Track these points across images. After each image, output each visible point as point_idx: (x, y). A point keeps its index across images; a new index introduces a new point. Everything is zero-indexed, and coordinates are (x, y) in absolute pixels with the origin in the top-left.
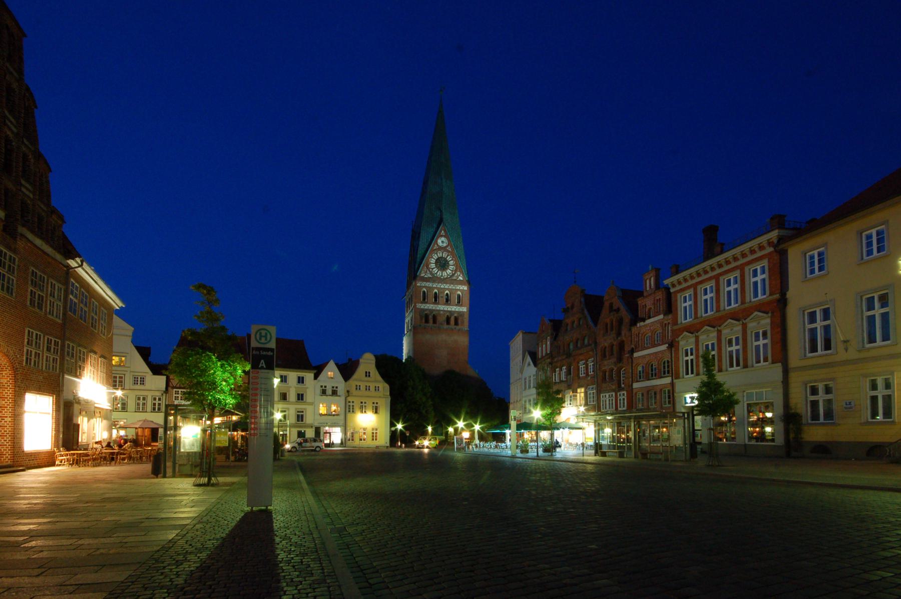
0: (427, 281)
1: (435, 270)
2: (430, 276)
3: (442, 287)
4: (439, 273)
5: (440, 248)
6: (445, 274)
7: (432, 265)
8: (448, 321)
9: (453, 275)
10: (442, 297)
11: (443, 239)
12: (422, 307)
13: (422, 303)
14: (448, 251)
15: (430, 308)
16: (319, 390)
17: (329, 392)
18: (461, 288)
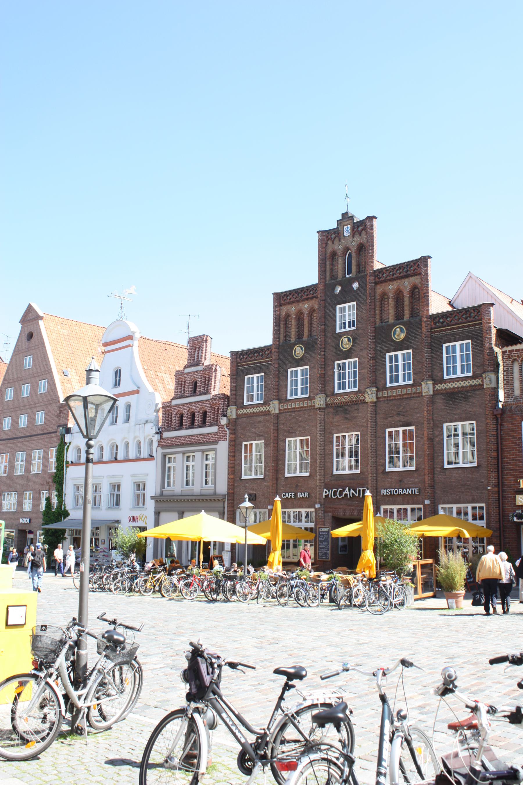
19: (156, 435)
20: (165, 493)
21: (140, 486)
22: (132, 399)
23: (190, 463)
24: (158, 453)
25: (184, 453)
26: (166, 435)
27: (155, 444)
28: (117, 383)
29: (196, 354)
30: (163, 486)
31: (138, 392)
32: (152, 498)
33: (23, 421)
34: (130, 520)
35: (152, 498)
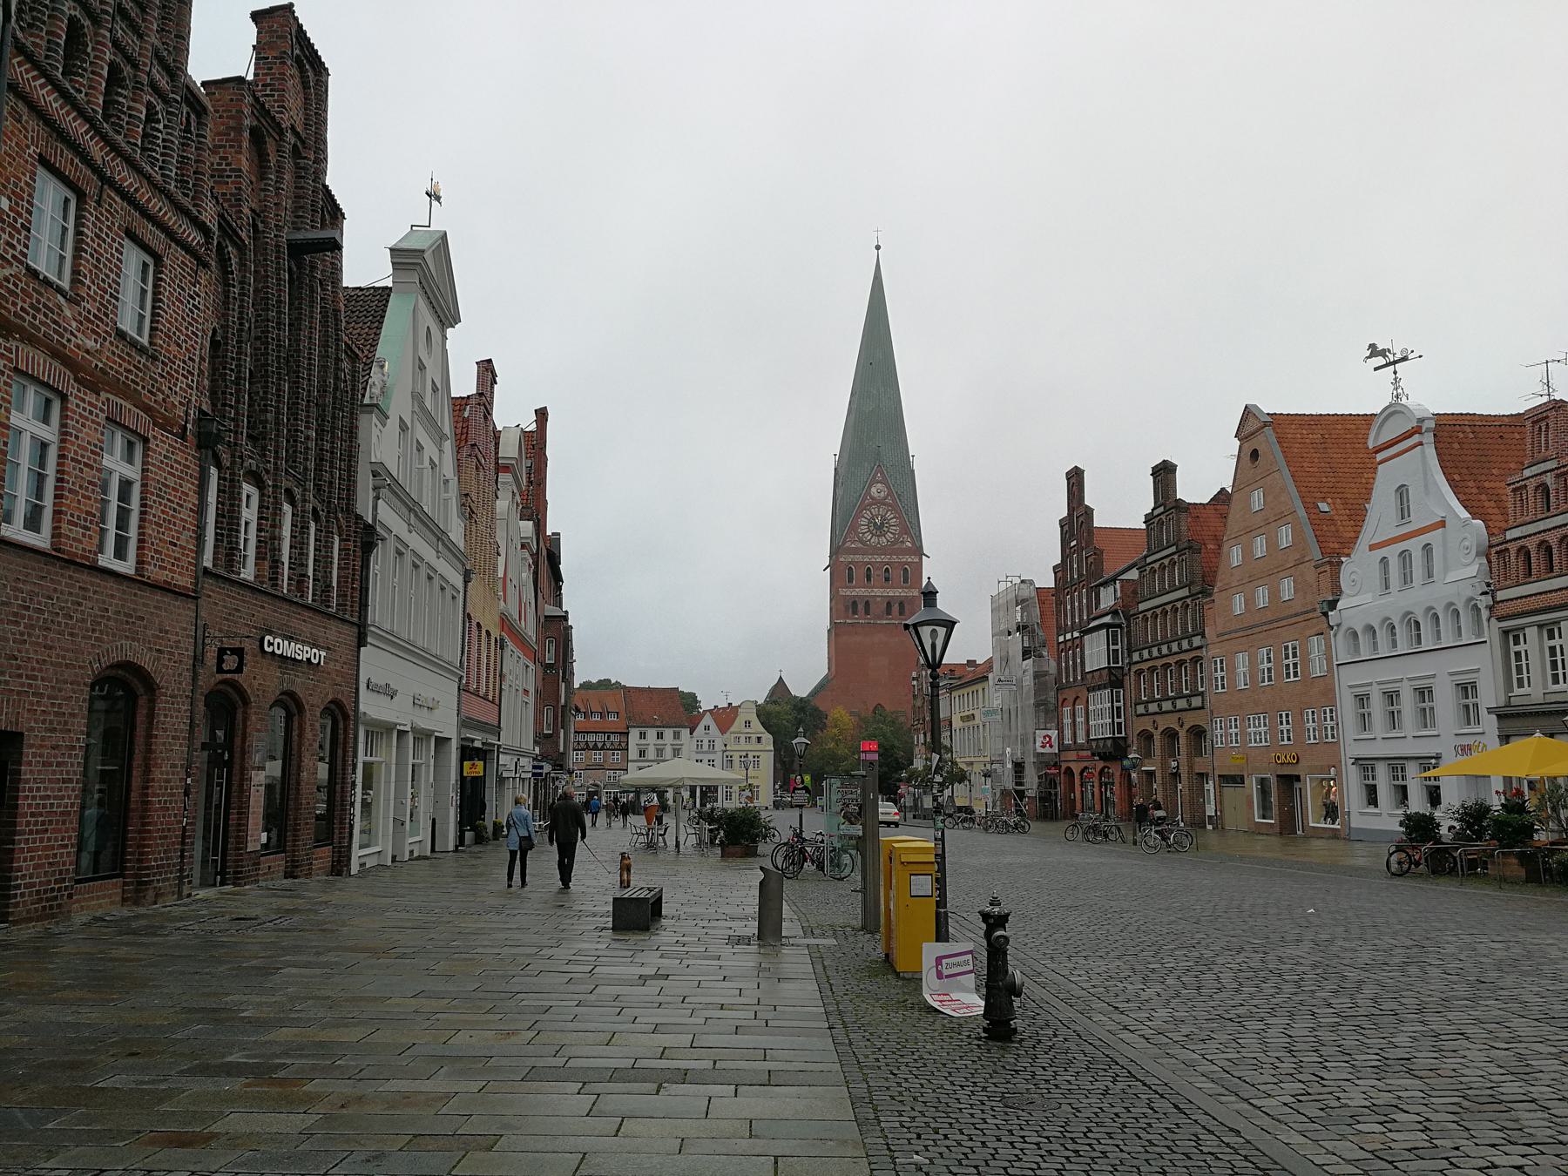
12: (848, 593)
19: (1483, 597)
20: (1514, 701)
21: (1467, 689)
22: (1434, 537)
23: (1556, 642)
24: (1492, 630)
25: (1540, 626)
26: (1500, 595)
27: (1485, 614)
28: (1404, 512)
29: (1543, 439)
30: (1509, 688)
31: (1442, 524)
32: (1490, 711)
33: (1262, 597)
34: (1457, 753)
35: (1490, 711)
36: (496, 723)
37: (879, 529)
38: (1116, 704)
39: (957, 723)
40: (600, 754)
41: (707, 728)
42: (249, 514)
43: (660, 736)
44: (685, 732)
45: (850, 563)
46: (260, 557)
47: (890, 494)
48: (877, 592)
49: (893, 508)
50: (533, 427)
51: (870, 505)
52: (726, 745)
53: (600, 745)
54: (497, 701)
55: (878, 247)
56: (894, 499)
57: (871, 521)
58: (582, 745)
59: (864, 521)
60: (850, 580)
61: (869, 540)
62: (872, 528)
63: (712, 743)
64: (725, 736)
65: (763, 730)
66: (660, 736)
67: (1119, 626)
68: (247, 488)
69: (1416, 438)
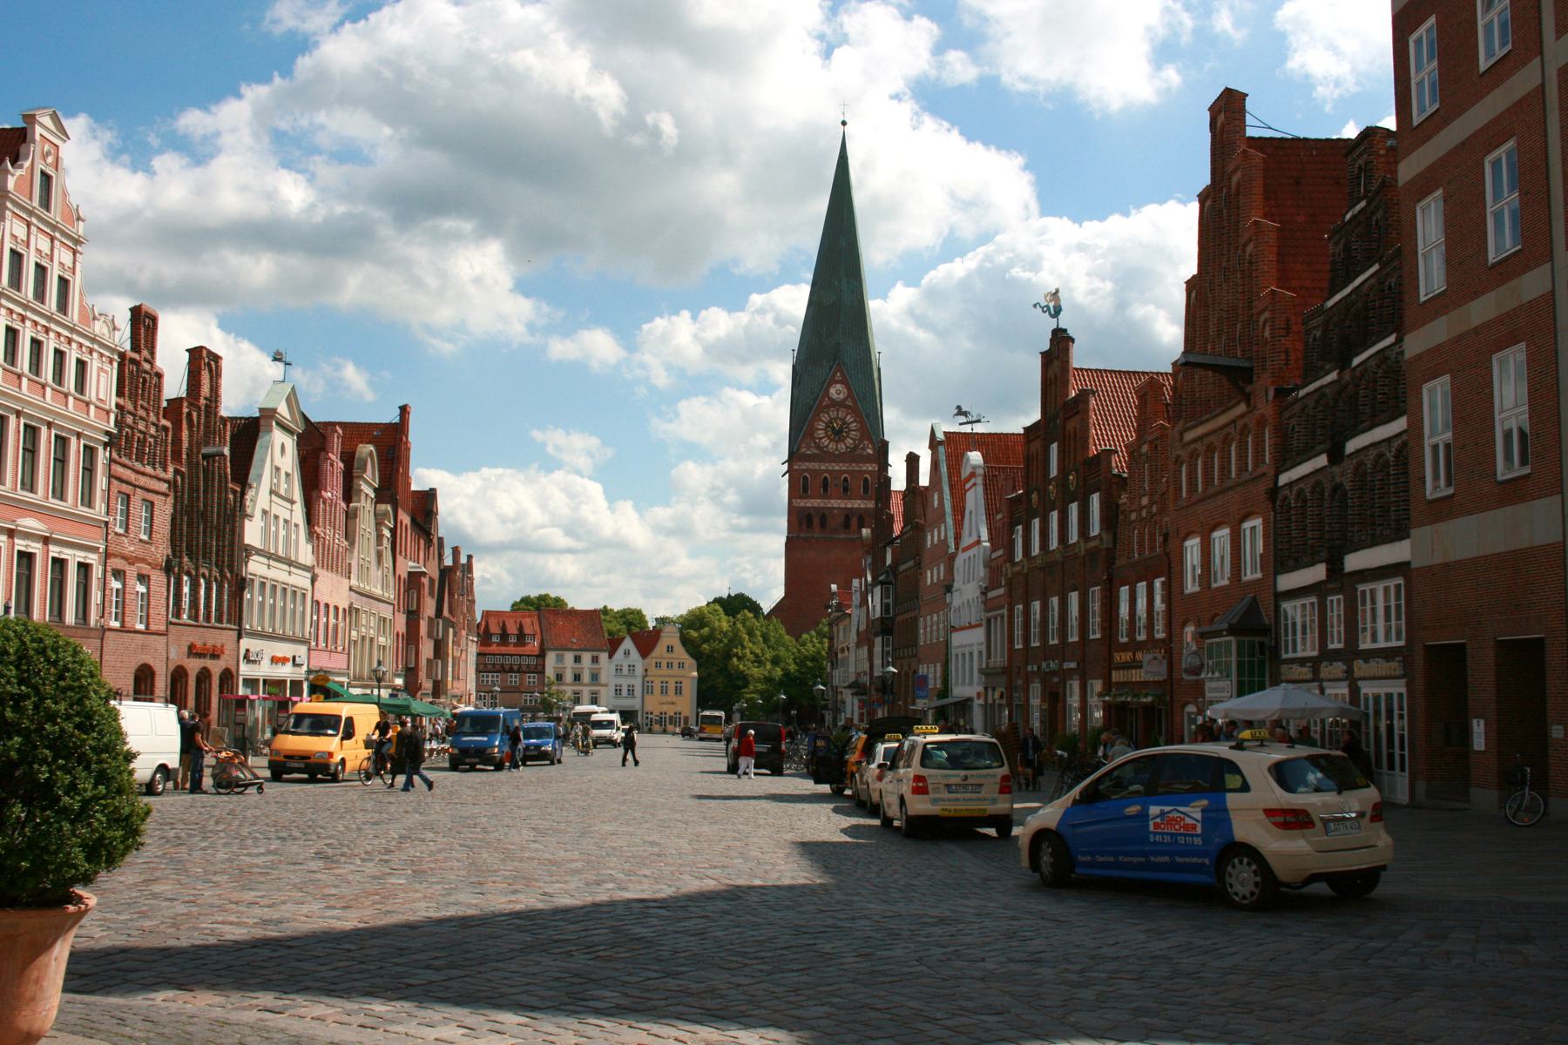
0: (813, 461)
1: (825, 442)
2: (816, 451)
3: (837, 468)
4: (832, 446)
5: (835, 404)
6: (842, 447)
7: (820, 432)
8: (846, 524)
9: (856, 447)
10: (836, 485)
11: (839, 386)
12: (802, 504)
13: (801, 498)
14: (848, 407)
15: (816, 505)
16: (613, 668)
17: (625, 671)
18: (870, 469)
26: (991, 594)
36: (345, 667)
37: (838, 434)
38: (886, 649)
39: (840, 656)
40: (516, 677)
41: (627, 653)
42: (186, 589)
43: (577, 659)
44: (604, 656)
45: (806, 470)
46: (190, 608)
47: (850, 395)
48: (834, 503)
49: (854, 410)
50: (397, 420)
51: (828, 407)
52: (646, 670)
53: (515, 668)
54: (347, 650)
55: (844, 123)
56: (855, 402)
57: (829, 425)
58: (498, 667)
59: (821, 425)
60: (805, 490)
61: (827, 446)
62: (830, 433)
63: (632, 667)
64: (648, 660)
65: (687, 656)
66: (577, 659)
67: (890, 583)
68: (185, 578)
69: (972, 481)
